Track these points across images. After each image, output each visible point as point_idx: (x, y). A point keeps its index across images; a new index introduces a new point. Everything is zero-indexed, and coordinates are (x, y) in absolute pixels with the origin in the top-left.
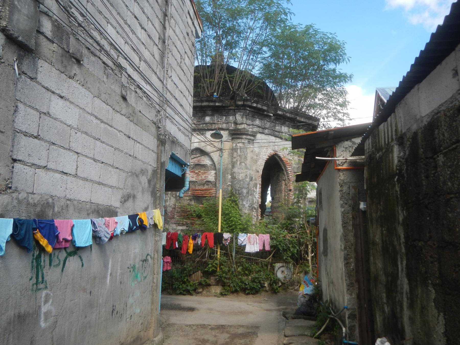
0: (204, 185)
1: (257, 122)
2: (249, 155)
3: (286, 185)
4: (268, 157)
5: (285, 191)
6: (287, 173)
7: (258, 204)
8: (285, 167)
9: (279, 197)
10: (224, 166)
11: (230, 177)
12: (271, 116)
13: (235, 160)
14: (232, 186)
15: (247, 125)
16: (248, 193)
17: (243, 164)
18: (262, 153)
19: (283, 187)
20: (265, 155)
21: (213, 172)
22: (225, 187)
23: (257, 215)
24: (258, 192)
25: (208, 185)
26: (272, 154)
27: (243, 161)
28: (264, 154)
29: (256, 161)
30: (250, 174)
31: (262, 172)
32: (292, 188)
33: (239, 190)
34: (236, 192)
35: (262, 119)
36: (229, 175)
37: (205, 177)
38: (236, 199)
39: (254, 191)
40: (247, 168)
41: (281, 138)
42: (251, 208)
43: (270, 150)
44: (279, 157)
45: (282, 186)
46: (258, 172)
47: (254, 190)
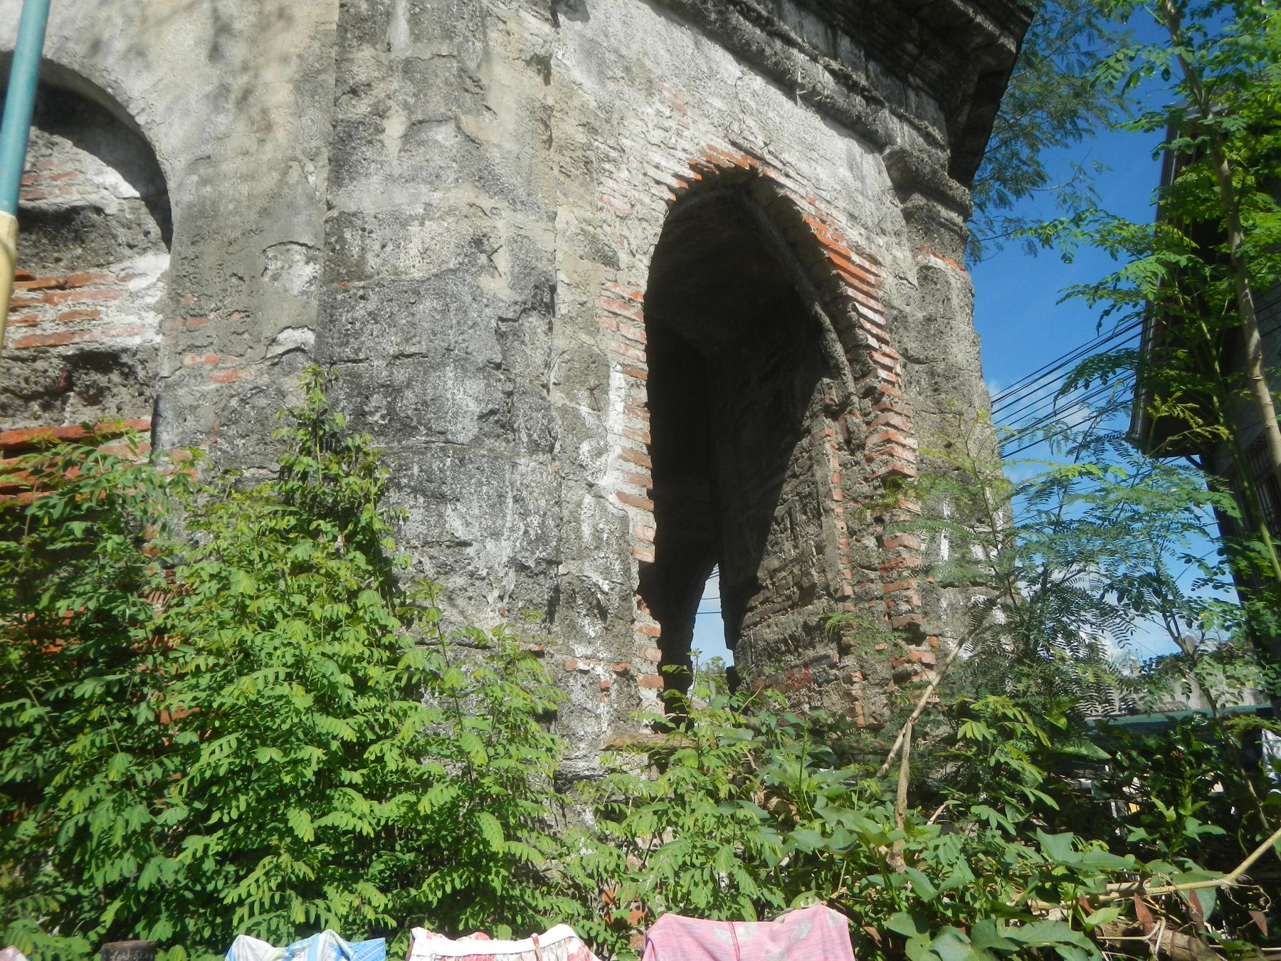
0: (53, 396)
2: (509, 84)
3: (851, 443)
4: (691, 175)
5: (846, 490)
6: (856, 349)
7: (624, 554)
8: (839, 305)
9: (801, 559)
10: (249, 177)
11: (309, 270)
13: (361, 108)
14: (322, 357)
16: (499, 420)
17: (444, 135)
18: (633, 124)
19: (834, 464)
21: (154, 266)
22: (252, 375)
23: (625, 676)
24: (618, 445)
25: (94, 397)
26: (725, 162)
27: (437, 105)
28: (657, 136)
29: (590, 168)
30: (520, 240)
31: (651, 269)
32: (905, 460)
33: (392, 390)
34: (360, 414)
36: (298, 254)
37: (67, 319)
38: (355, 482)
39: (576, 427)
40: (485, 179)
41: (782, 79)
42: (541, 593)
43: (704, 125)
44: (785, 211)
45: (816, 460)
46: (610, 261)
47: (569, 414)
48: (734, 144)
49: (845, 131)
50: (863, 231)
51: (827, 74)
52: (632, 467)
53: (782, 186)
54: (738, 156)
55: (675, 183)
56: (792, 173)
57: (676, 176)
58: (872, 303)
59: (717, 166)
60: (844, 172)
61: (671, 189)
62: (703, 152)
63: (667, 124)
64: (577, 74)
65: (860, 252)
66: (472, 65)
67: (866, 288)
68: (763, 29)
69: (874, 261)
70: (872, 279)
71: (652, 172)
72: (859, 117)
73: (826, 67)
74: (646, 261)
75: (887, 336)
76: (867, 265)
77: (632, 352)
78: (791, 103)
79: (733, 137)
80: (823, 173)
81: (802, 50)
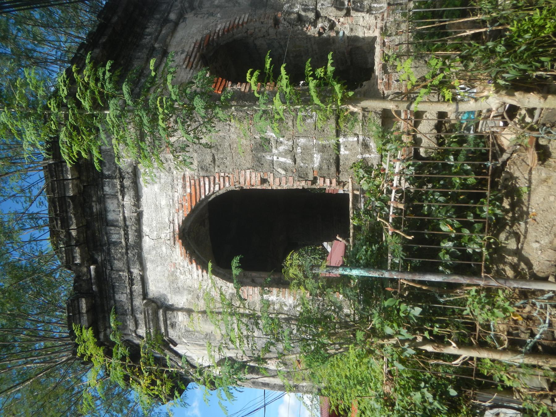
1: (122, 297)
4: (194, 264)
12: (96, 270)
15: (137, 328)
20: (190, 272)
26: (183, 250)
28: (189, 276)
35: (113, 287)
48: (174, 244)
49: (139, 185)
50: (175, 182)
51: (125, 199)
52: (287, 295)
53: (179, 226)
54: (179, 243)
55: (200, 271)
56: (171, 219)
57: (197, 269)
58: (202, 183)
59: (186, 253)
60: (156, 187)
61: (202, 272)
62: (185, 258)
63: (183, 271)
64: (185, 300)
65: (184, 187)
66: (203, 336)
67: (198, 187)
68: (128, 231)
69: (184, 178)
70: (192, 181)
71: (201, 278)
72: (132, 183)
73: (123, 200)
74: (228, 283)
75: (212, 178)
76: (188, 184)
77: (256, 292)
78: (144, 213)
79: (172, 243)
80: (164, 202)
81: (124, 213)
